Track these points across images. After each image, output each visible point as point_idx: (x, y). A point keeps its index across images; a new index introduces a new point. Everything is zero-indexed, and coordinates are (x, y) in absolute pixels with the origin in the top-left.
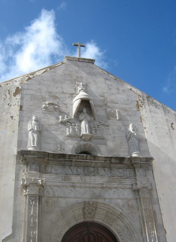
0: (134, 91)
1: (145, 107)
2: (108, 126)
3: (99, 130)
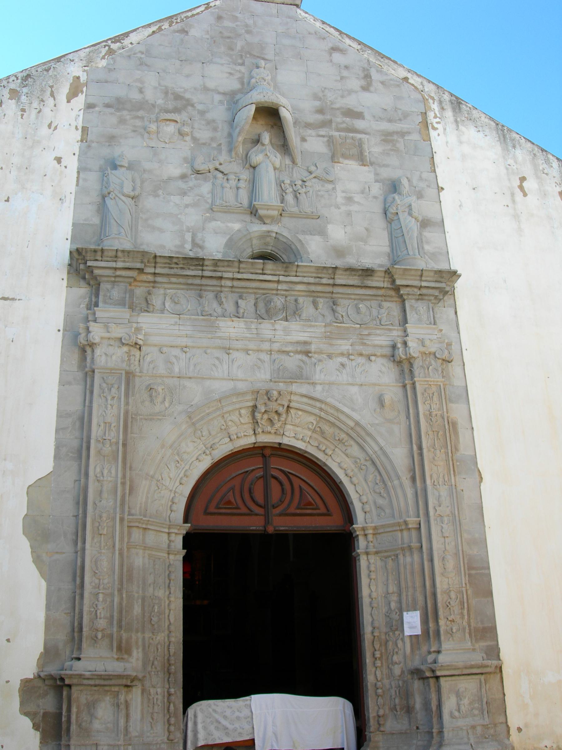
0: (416, 85)
1: (445, 129)
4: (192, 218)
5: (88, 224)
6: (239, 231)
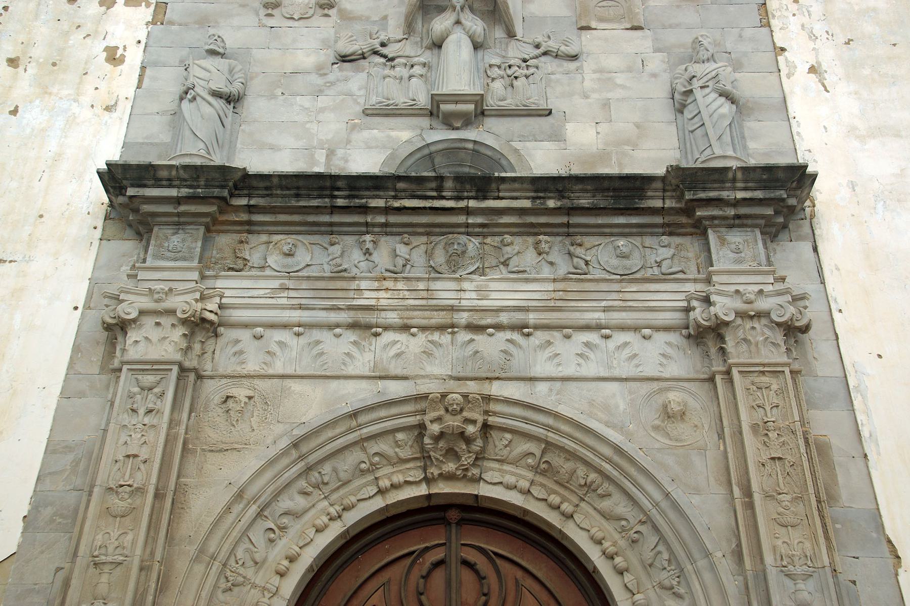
2: (574, 57)
3: (527, 77)
5: (151, 144)
6: (408, 141)
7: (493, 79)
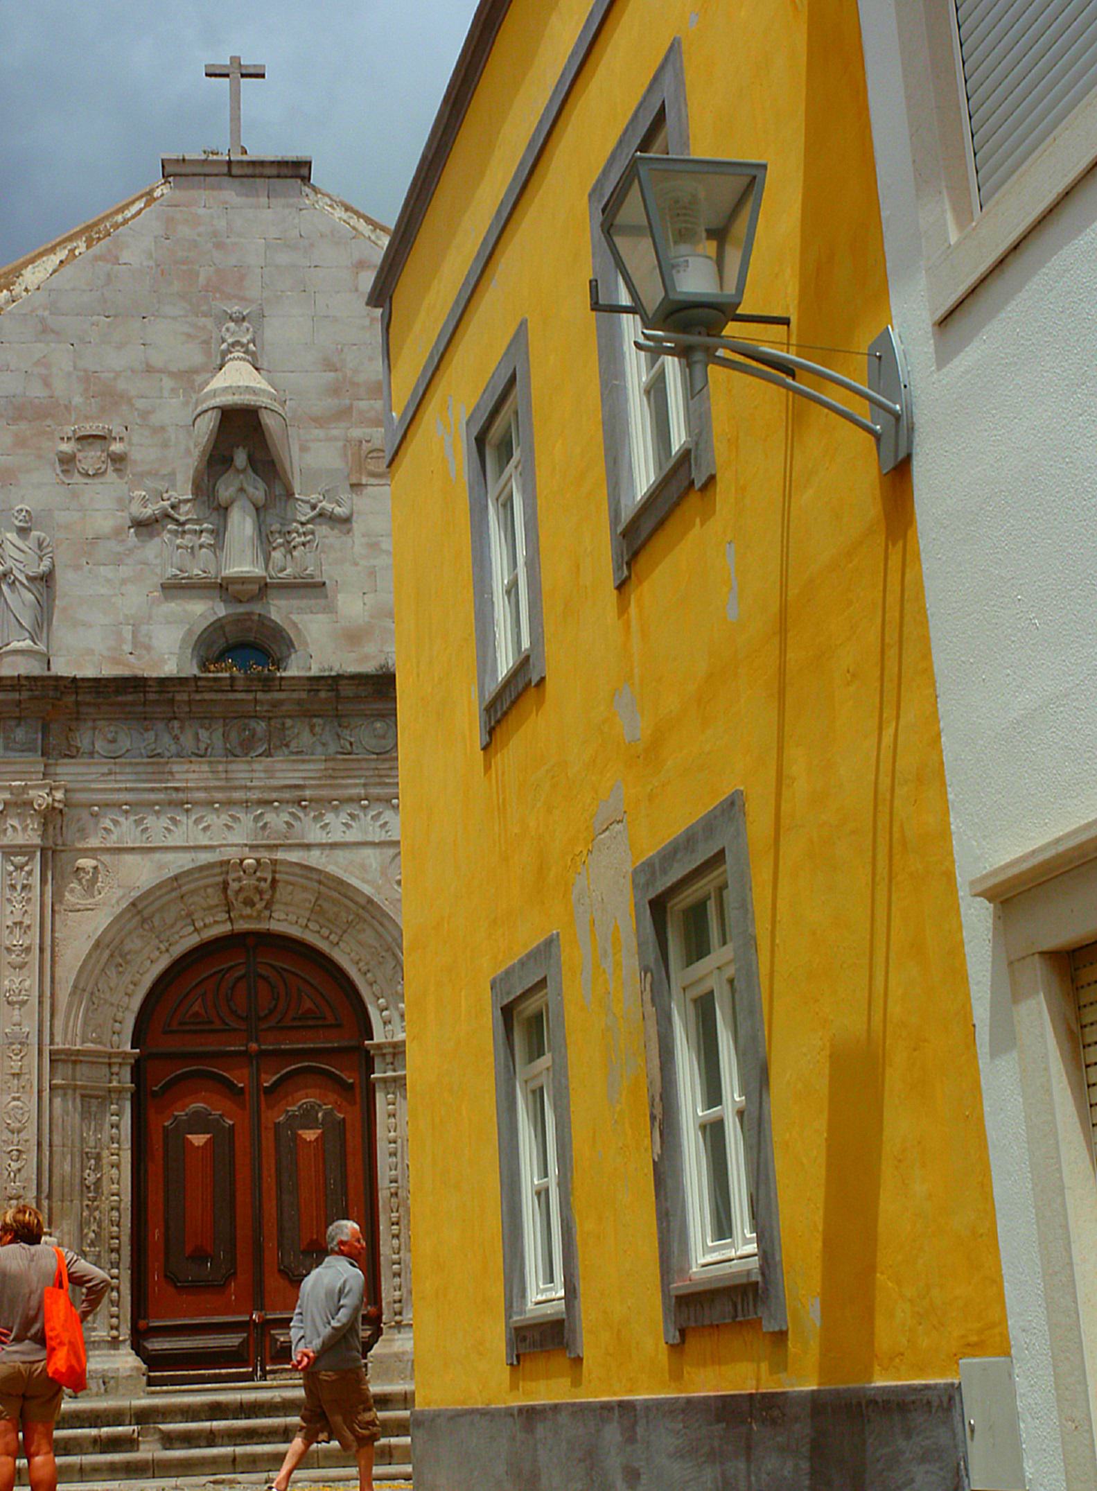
3: (304, 544)
4: (135, 599)
7: (274, 549)
